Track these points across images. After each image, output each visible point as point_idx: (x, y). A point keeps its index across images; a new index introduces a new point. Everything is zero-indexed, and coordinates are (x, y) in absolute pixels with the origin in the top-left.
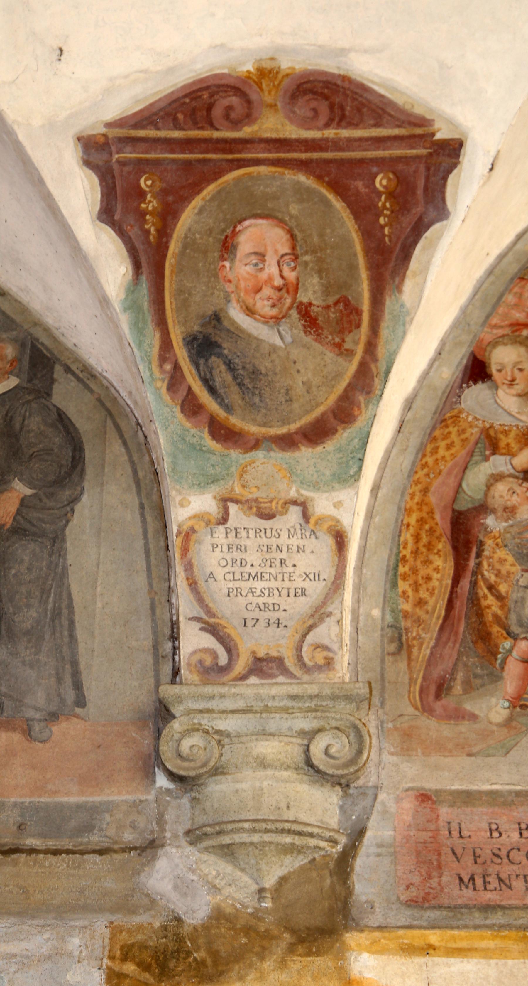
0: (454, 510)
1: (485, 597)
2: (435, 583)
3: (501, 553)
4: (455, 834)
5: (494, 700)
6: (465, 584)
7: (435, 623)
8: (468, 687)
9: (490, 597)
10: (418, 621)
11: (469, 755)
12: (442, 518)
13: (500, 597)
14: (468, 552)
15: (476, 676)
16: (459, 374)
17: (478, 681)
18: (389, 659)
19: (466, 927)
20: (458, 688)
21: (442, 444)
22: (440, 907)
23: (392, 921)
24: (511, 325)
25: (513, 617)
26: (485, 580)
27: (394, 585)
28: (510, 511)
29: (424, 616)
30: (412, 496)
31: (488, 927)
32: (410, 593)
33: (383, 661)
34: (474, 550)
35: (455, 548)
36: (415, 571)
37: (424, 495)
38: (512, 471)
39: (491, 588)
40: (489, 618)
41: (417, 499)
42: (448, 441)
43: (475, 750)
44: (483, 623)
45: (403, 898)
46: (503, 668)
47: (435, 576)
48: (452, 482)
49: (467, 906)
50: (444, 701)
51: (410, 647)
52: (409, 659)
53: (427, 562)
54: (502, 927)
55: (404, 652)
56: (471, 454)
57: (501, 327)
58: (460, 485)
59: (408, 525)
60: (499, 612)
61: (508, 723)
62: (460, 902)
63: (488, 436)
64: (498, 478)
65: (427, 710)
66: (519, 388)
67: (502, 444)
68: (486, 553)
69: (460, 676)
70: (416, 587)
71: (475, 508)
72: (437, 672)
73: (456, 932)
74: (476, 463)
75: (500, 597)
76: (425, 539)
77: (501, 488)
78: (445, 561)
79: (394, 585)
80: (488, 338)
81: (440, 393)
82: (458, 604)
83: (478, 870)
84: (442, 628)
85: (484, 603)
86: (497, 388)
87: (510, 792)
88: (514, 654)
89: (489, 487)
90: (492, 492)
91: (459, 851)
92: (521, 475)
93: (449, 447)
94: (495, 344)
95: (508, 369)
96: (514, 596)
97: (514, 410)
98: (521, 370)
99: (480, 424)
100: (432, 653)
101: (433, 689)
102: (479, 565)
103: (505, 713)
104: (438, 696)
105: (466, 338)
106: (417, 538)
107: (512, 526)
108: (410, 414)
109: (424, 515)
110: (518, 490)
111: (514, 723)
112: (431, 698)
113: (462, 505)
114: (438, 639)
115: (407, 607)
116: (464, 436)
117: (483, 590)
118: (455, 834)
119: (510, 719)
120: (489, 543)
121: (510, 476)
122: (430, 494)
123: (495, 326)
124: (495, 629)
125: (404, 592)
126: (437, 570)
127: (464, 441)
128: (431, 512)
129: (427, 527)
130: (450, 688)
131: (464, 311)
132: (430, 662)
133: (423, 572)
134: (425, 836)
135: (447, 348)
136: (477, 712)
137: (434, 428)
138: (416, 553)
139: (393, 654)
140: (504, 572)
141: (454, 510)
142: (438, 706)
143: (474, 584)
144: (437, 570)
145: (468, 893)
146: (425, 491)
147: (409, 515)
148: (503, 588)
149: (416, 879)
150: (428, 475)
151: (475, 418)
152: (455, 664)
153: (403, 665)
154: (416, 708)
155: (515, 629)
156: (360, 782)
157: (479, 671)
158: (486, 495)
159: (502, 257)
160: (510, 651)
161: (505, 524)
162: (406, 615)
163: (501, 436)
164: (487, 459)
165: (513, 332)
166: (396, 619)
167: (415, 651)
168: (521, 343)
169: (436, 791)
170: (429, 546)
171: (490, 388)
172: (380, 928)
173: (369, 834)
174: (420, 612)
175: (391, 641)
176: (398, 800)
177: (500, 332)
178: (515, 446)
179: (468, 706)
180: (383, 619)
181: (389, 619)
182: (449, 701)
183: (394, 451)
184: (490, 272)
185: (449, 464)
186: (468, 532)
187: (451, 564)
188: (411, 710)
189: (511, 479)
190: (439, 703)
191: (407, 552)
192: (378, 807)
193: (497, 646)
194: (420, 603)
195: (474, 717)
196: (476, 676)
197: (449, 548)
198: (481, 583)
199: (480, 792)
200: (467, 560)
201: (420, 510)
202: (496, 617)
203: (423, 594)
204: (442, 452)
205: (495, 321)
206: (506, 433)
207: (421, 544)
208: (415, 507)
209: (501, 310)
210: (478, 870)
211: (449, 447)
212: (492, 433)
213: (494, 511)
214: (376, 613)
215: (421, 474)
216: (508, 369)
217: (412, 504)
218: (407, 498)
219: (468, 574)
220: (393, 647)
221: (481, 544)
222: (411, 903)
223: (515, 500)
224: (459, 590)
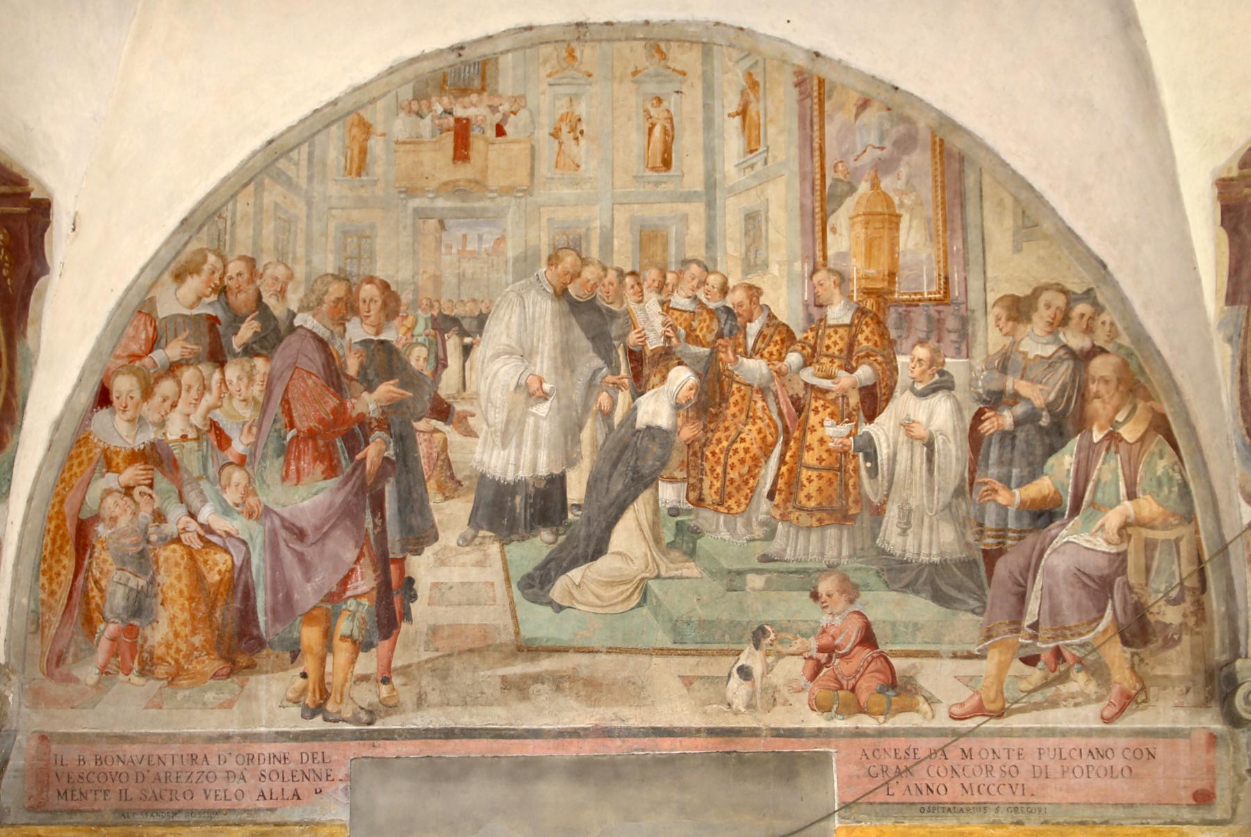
0: (79, 519)
1: (92, 590)
2: (62, 578)
3: (105, 555)
4: (59, 763)
5: (90, 668)
6: (81, 578)
7: (60, 609)
8: (77, 658)
9: (95, 590)
10: (50, 608)
11: (72, 708)
12: (71, 525)
13: (101, 590)
14: (85, 554)
15: (81, 650)
16: (92, 400)
17: (83, 654)
18: (30, 636)
19: (59, 824)
20: (70, 659)
21: (76, 462)
22: (46, 811)
23: (19, 821)
24: (129, 356)
25: (107, 605)
26: (93, 576)
27: (37, 579)
28: (114, 519)
29: (54, 604)
30: (53, 506)
31: (72, 824)
32: (47, 586)
33: (26, 638)
34: (89, 552)
35: (77, 550)
36: (50, 568)
37: (61, 506)
38: (118, 487)
39: (96, 582)
40: (93, 606)
41: (56, 510)
42: (79, 460)
43: (75, 704)
44: (89, 610)
45: (26, 806)
46: (97, 645)
47: (63, 572)
48: (79, 497)
49: (61, 811)
50: (60, 669)
51: (43, 627)
52: (42, 637)
53: (59, 561)
54: (79, 824)
55: (39, 632)
56: (93, 471)
57: (123, 358)
58: (84, 498)
59: (49, 531)
60: (100, 602)
61: (97, 686)
62: (57, 808)
63: (106, 457)
64: (108, 492)
65: (50, 675)
66: (129, 414)
67: (114, 464)
68: (96, 555)
69: (72, 650)
70: (51, 580)
71: (92, 517)
72: (58, 648)
73: (53, 827)
74: (96, 479)
75: (101, 590)
76: (59, 543)
77: (110, 501)
78: (70, 560)
79: (37, 579)
80: (113, 367)
81: (78, 416)
82: (75, 594)
83: (70, 787)
84: (64, 614)
85: (91, 594)
86: (114, 413)
87: (93, 734)
88: (106, 634)
89: (102, 499)
90: (103, 505)
91: (60, 775)
92: (123, 490)
93: (80, 464)
94: (117, 373)
95: (124, 396)
96: (110, 589)
97: (124, 434)
98: (132, 398)
99: (101, 444)
100: (56, 633)
101: (55, 659)
102: (90, 563)
103: (96, 677)
104: (57, 665)
105: (98, 367)
106: (54, 541)
107: (113, 533)
108: (57, 435)
109: (59, 522)
110: (121, 503)
111: (100, 685)
112: (53, 666)
113: (84, 516)
114: (61, 622)
115: (43, 596)
116: (90, 455)
117: (91, 584)
118: (59, 763)
119: (99, 682)
120: (99, 546)
121: (116, 491)
122: (65, 505)
123: (118, 357)
124: (96, 615)
125: (43, 585)
126: (64, 567)
127: (90, 459)
128: (64, 520)
129: (61, 532)
130: (65, 659)
131: (99, 342)
132: (56, 638)
133: (55, 570)
134: (42, 764)
135: (86, 375)
136: (80, 677)
137: (72, 448)
138: (52, 553)
139: (34, 633)
140: (105, 570)
141: (79, 519)
142: (57, 672)
143: (86, 579)
144: (64, 567)
145: (62, 802)
146: (62, 502)
147: (50, 522)
148: (103, 583)
149: (34, 793)
150: (64, 489)
151: (99, 440)
152: (70, 641)
153: (38, 642)
154: (44, 674)
155: (108, 615)
156: (7, 727)
157: (83, 646)
158: (100, 507)
159: (128, 290)
160: (103, 632)
161: (109, 531)
162: (43, 602)
163: (114, 456)
164: (103, 476)
165: (130, 362)
166: (37, 606)
167: (46, 630)
168: (134, 374)
169: (51, 733)
170: (61, 548)
171: (111, 413)
172: (12, 825)
173: (10, 763)
174: (52, 601)
175: (32, 623)
176: (28, 739)
177: (121, 362)
178: (122, 465)
179: (75, 673)
180: (29, 606)
181: (32, 606)
182: (64, 668)
183: (45, 468)
184: (119, 305)
185: (79, 479)
186: (86, 537)
187: (73, 562)
188: (40, 675)
189: (117, 494)
190: (58, 670)
191: (47, 553)
192: (16, 744)
193: (96, 628)
194: (52, 593)
195: (77, 680)
196: (81, 650)
197: (73, 550)
198: (91, 579)
199: (76, 734)
200: (83, 560)
201: (58, 518)
202: (98, 605)
203: (55, 587)
204: (75, 468)
205: (118, 352)
206: (117, 453)
207: (56, 546)
208: (54, 515)
209: (124, 341)
210: (70, 787)
211: (80, 464)
212: (108, 453)
213: (103, 520)
214: (25, 601)
215: (61, 486)
216: (124, 396)
217: (53, 513)
218: (50, 508)
219: (83, 571)
220: (33, 628)
221: (94, 547)
222: (32, 809)
223: (118, 511)
224: (76, 583)
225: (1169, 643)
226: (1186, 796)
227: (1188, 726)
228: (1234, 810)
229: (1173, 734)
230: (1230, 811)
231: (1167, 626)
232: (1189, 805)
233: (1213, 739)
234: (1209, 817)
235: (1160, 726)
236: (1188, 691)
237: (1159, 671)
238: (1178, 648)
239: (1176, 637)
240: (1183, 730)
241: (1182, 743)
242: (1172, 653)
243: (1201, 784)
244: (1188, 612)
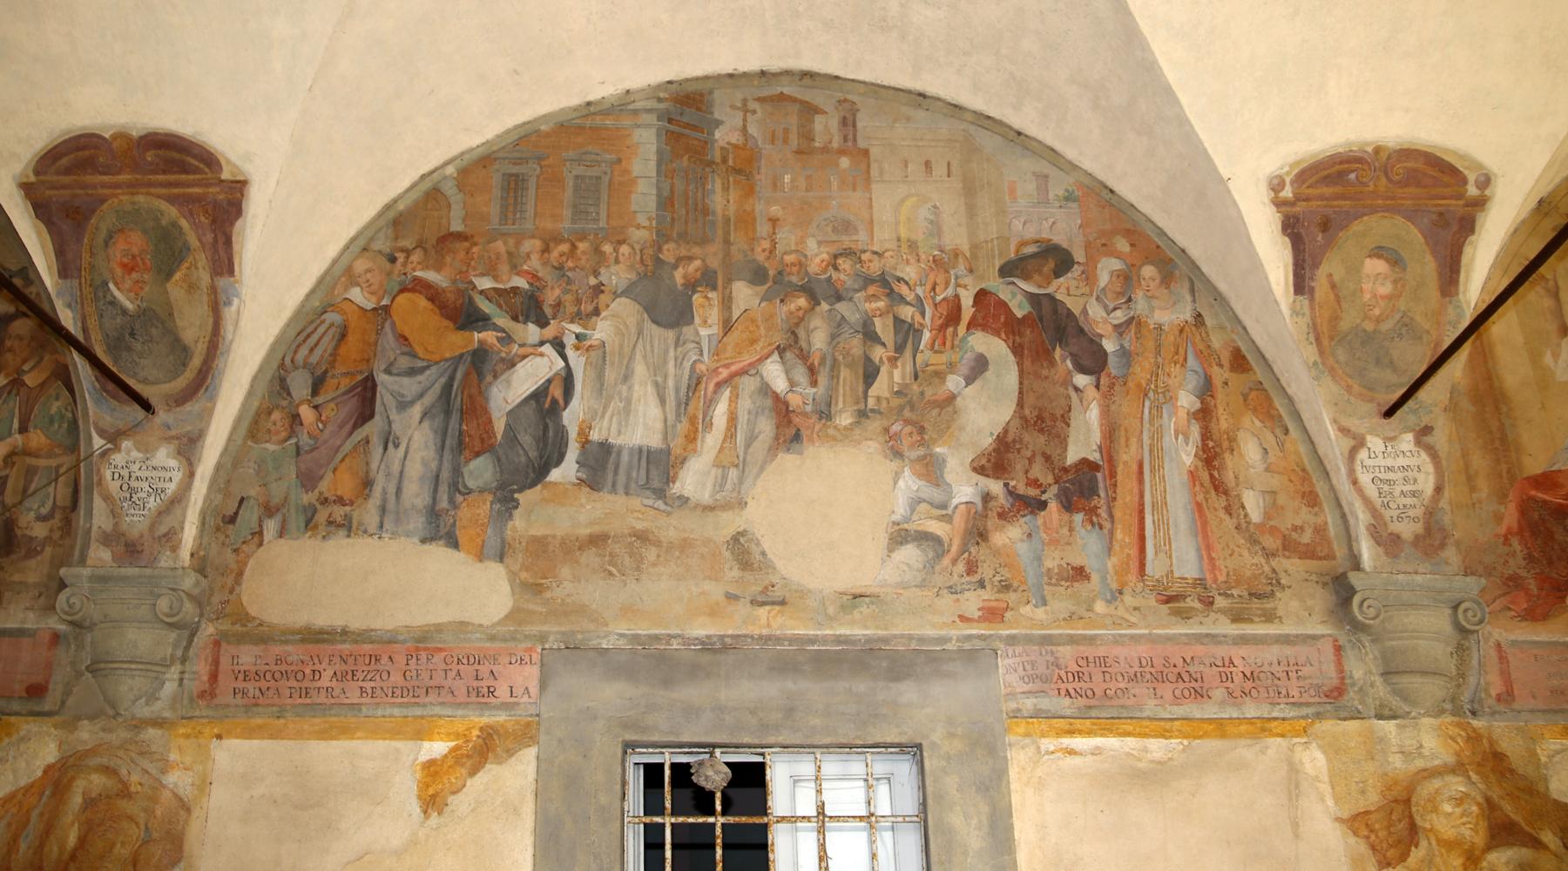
225: (32, 553)
226: (19, 688)
227: (35, 627)
228: (63, 703)
229: (20, 633)
230: (59, 703)
231: (31, 539)
232: (20, 698)
233: (56, 638)
234: (37, 709)
235: (8, 626)
236: (40, 595)
237: (16, 578)
238: (39, 558)
239: (39, 548)
240: (29, 629)
241: (26, 642)
242: (32, 563)
243: (37, 679)
244: (55, 527)
